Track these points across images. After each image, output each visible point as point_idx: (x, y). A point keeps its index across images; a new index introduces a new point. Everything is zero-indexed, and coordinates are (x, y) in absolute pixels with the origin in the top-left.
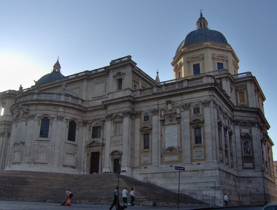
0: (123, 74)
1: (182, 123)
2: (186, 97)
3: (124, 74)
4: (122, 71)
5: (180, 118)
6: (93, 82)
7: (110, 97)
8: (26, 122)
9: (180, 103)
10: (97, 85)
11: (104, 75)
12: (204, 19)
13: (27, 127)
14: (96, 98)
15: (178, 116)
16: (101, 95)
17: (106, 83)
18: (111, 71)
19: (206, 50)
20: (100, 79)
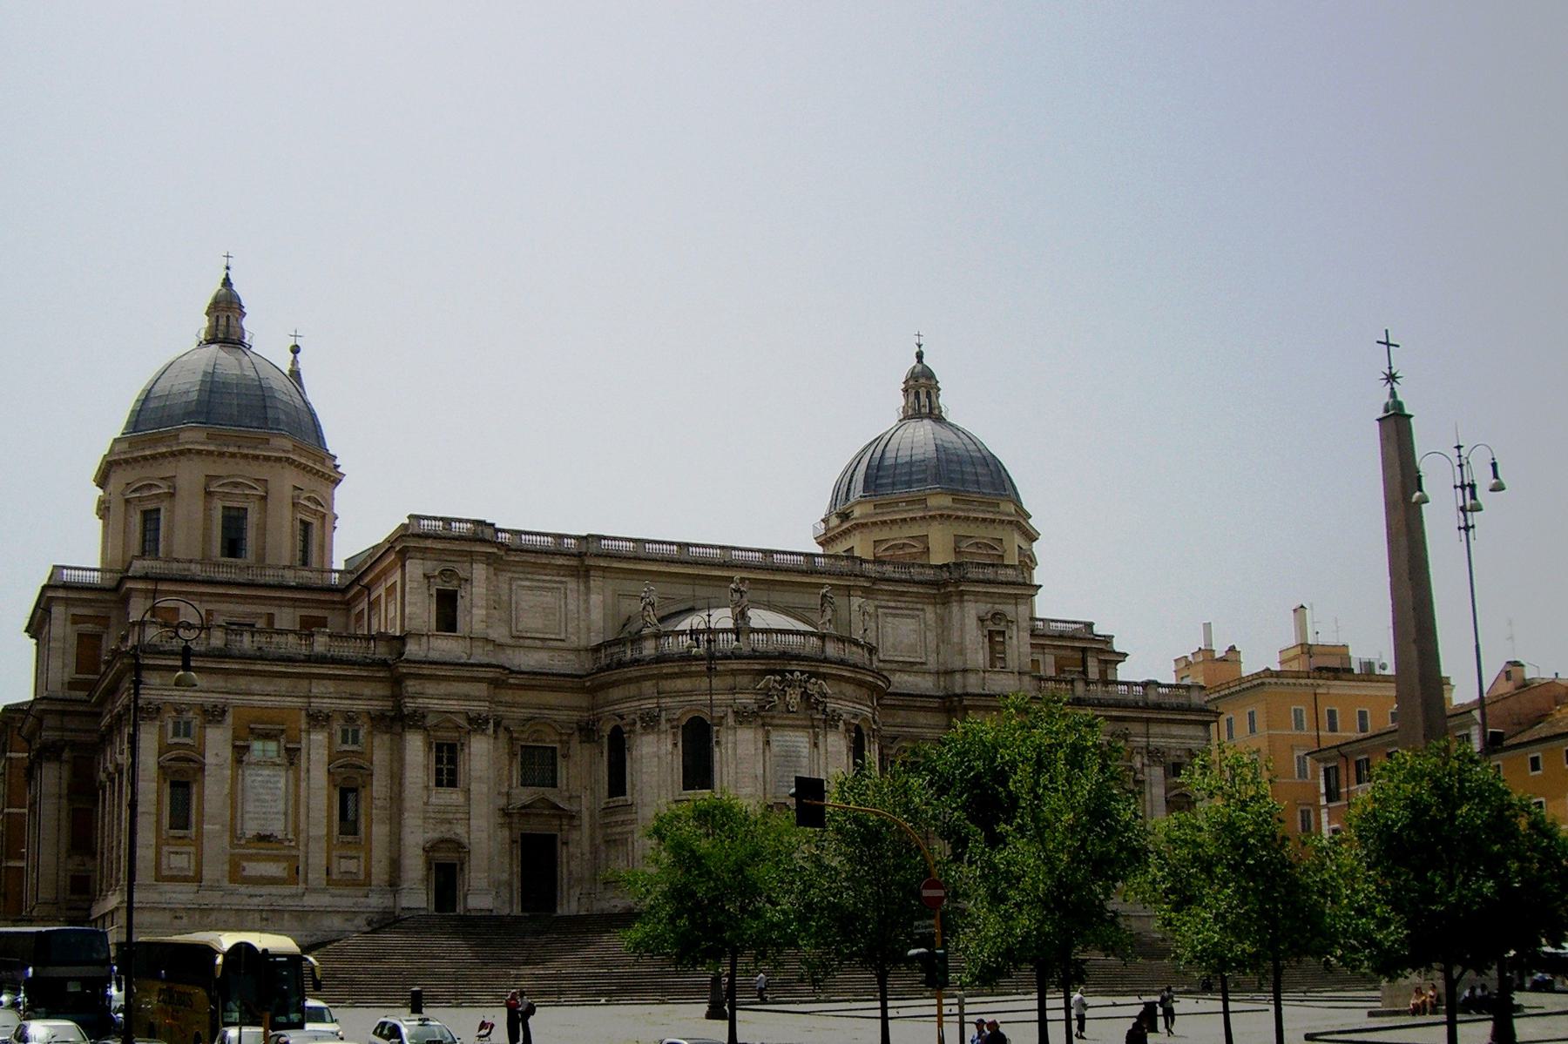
0: (1008, 621)
1: (1148, 797)
2: (1154, 729)
3: (1012, 622)
4: (1008, 609)
5: (1143, 781)
6: (876, 603)
7: (973, 684)
8: (816, 736)
9: (1142, 741)
10: (889, 619)
11: (929, 596)
12: (929, 375)
13: (819, 754)
14: (894, 666)
15: (1139, 776)
16: (912, 660)
17: (925, 623)
18: (966, 597)
19: (1008, 528)
20: (900, 598)
